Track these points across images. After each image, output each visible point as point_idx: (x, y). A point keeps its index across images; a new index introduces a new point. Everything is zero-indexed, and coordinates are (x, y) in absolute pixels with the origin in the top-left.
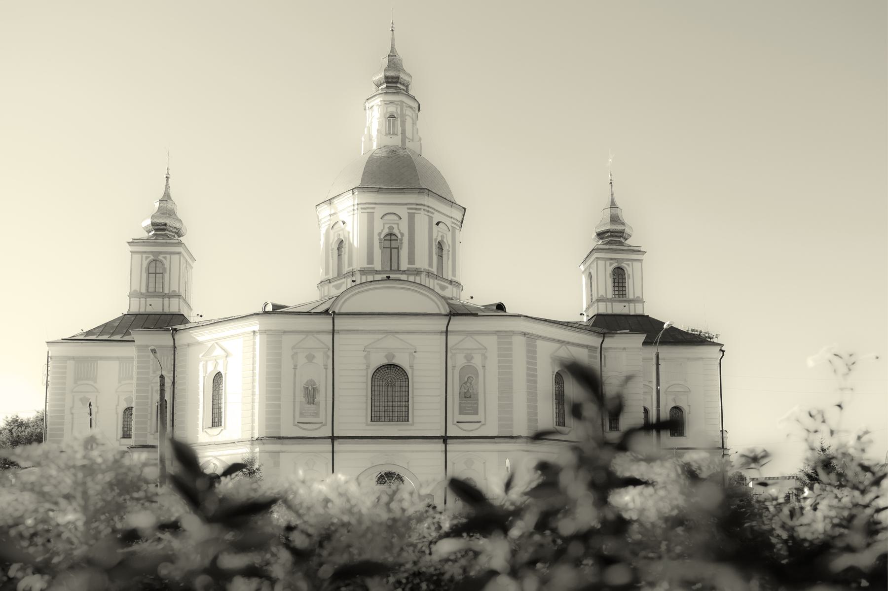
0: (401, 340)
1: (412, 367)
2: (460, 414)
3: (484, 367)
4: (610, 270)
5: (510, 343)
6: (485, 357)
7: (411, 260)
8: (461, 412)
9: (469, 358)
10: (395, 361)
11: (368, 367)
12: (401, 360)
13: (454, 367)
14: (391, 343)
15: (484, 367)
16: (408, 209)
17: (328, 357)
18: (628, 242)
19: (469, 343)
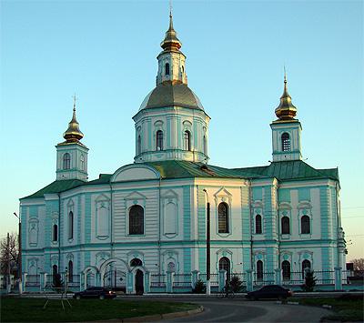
4: (280, 135)
7: (168, 145)
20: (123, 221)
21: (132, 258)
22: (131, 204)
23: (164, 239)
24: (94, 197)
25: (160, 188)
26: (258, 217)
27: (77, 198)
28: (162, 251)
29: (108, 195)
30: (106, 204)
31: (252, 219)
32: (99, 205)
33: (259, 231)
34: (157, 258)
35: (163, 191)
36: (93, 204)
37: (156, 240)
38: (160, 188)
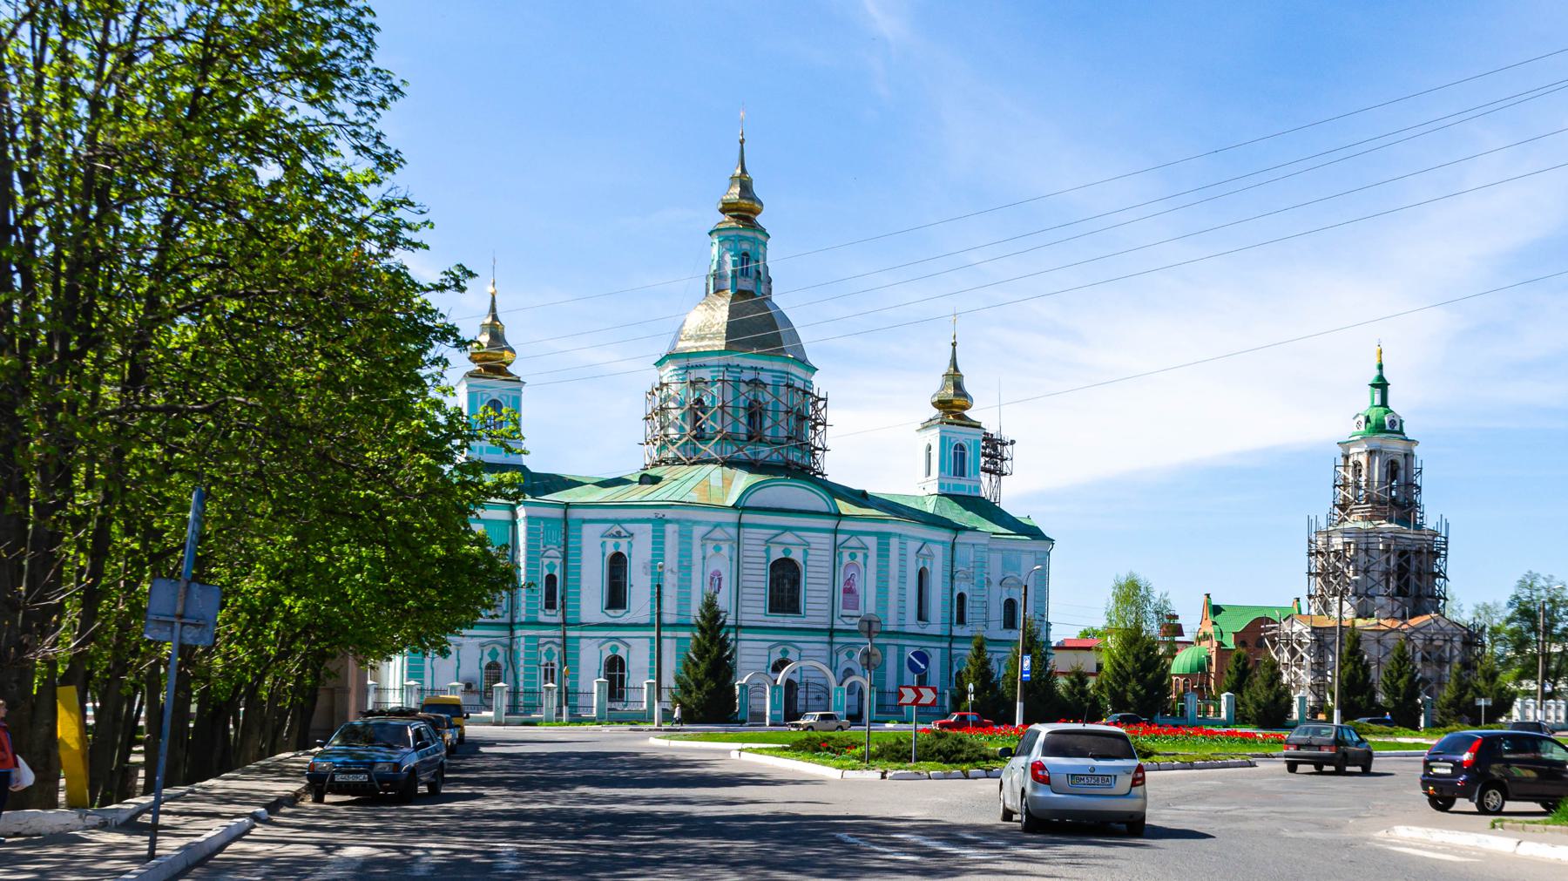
0: (798, 536)
1: (805, 562)
2: (844, 608)
3: (865, 565)
5: (889, 544)
6: (866, 556)
8: (844, 608)
9: (853, 556)
10: (791, 556)
11: (768, 561)
12: (796, 555)
13: (840, 563)
14: (788, 537)
15: (865, 565)
16: (773, 376)
17: (733, 549)
18: (966, 413)
19: (853, 542)
20: (758, 583)
21: (776, 656)
22: (777, 553)
23: (839, 624)
24: (698, 531)
25: (835, 532)
26: (961, 597)
27: (649, 526)
28: (836, 647)
29: (733, 531)
30: (726, 548)
31: (952, 600)
32: (710, 551)
33: (961, 620)
34: (825, 653)
35: (841, 538)
36: (697, 543)
37: (825, 627)
38: (835, 532)
